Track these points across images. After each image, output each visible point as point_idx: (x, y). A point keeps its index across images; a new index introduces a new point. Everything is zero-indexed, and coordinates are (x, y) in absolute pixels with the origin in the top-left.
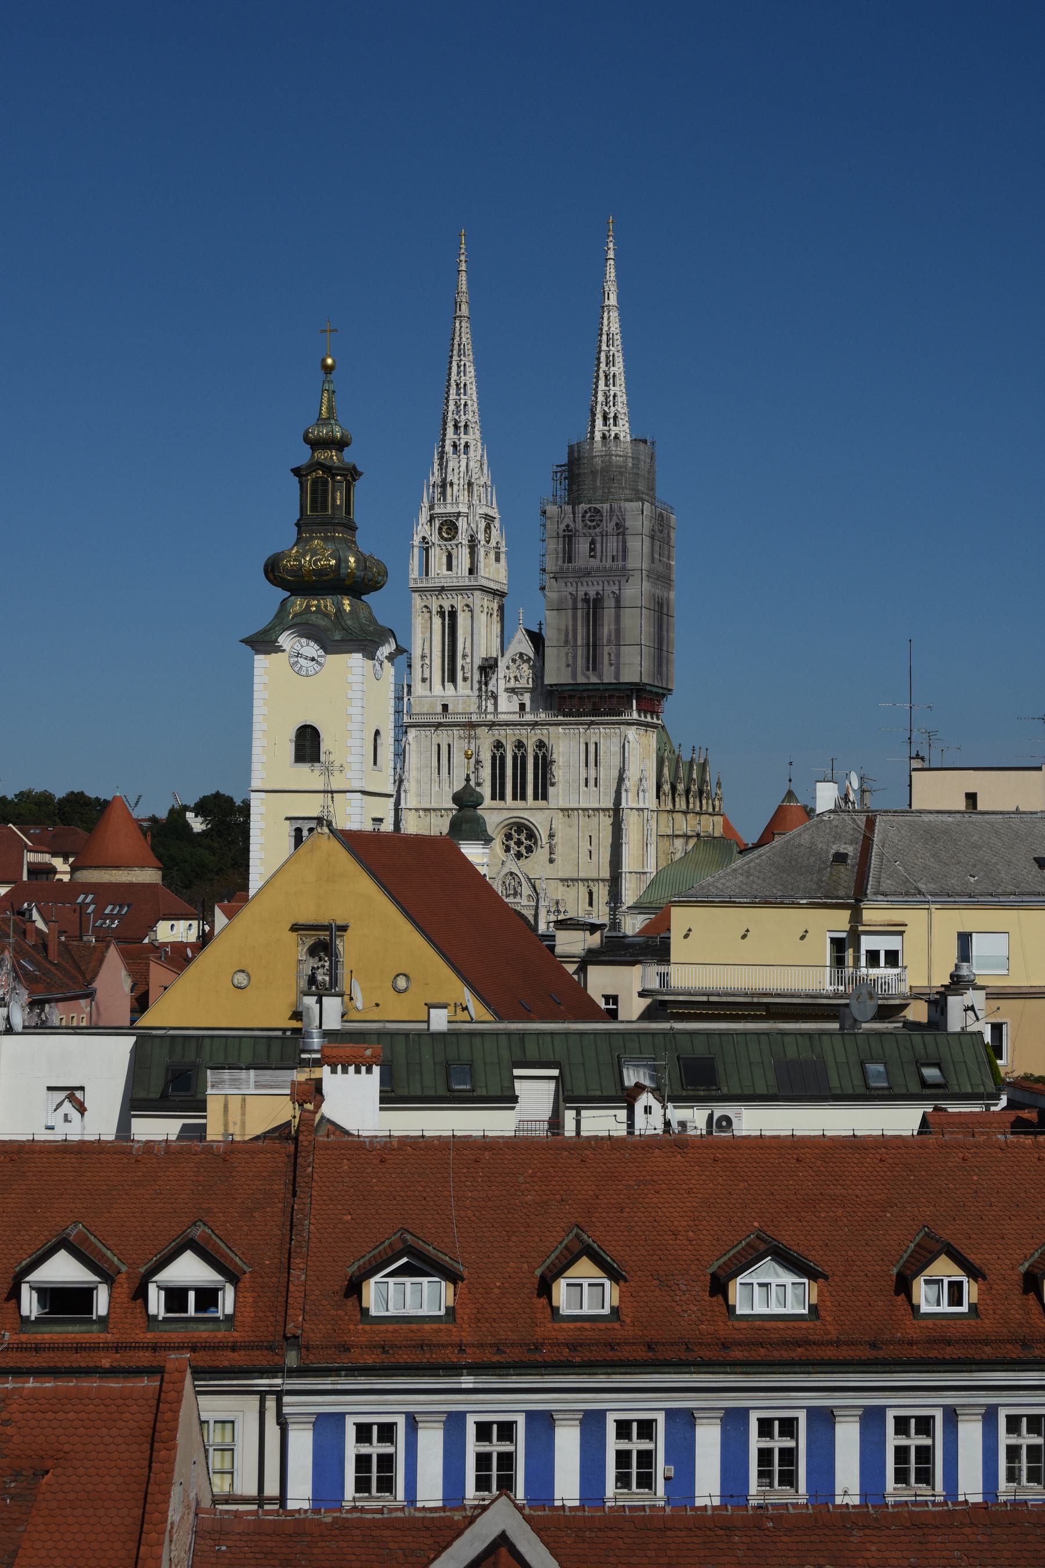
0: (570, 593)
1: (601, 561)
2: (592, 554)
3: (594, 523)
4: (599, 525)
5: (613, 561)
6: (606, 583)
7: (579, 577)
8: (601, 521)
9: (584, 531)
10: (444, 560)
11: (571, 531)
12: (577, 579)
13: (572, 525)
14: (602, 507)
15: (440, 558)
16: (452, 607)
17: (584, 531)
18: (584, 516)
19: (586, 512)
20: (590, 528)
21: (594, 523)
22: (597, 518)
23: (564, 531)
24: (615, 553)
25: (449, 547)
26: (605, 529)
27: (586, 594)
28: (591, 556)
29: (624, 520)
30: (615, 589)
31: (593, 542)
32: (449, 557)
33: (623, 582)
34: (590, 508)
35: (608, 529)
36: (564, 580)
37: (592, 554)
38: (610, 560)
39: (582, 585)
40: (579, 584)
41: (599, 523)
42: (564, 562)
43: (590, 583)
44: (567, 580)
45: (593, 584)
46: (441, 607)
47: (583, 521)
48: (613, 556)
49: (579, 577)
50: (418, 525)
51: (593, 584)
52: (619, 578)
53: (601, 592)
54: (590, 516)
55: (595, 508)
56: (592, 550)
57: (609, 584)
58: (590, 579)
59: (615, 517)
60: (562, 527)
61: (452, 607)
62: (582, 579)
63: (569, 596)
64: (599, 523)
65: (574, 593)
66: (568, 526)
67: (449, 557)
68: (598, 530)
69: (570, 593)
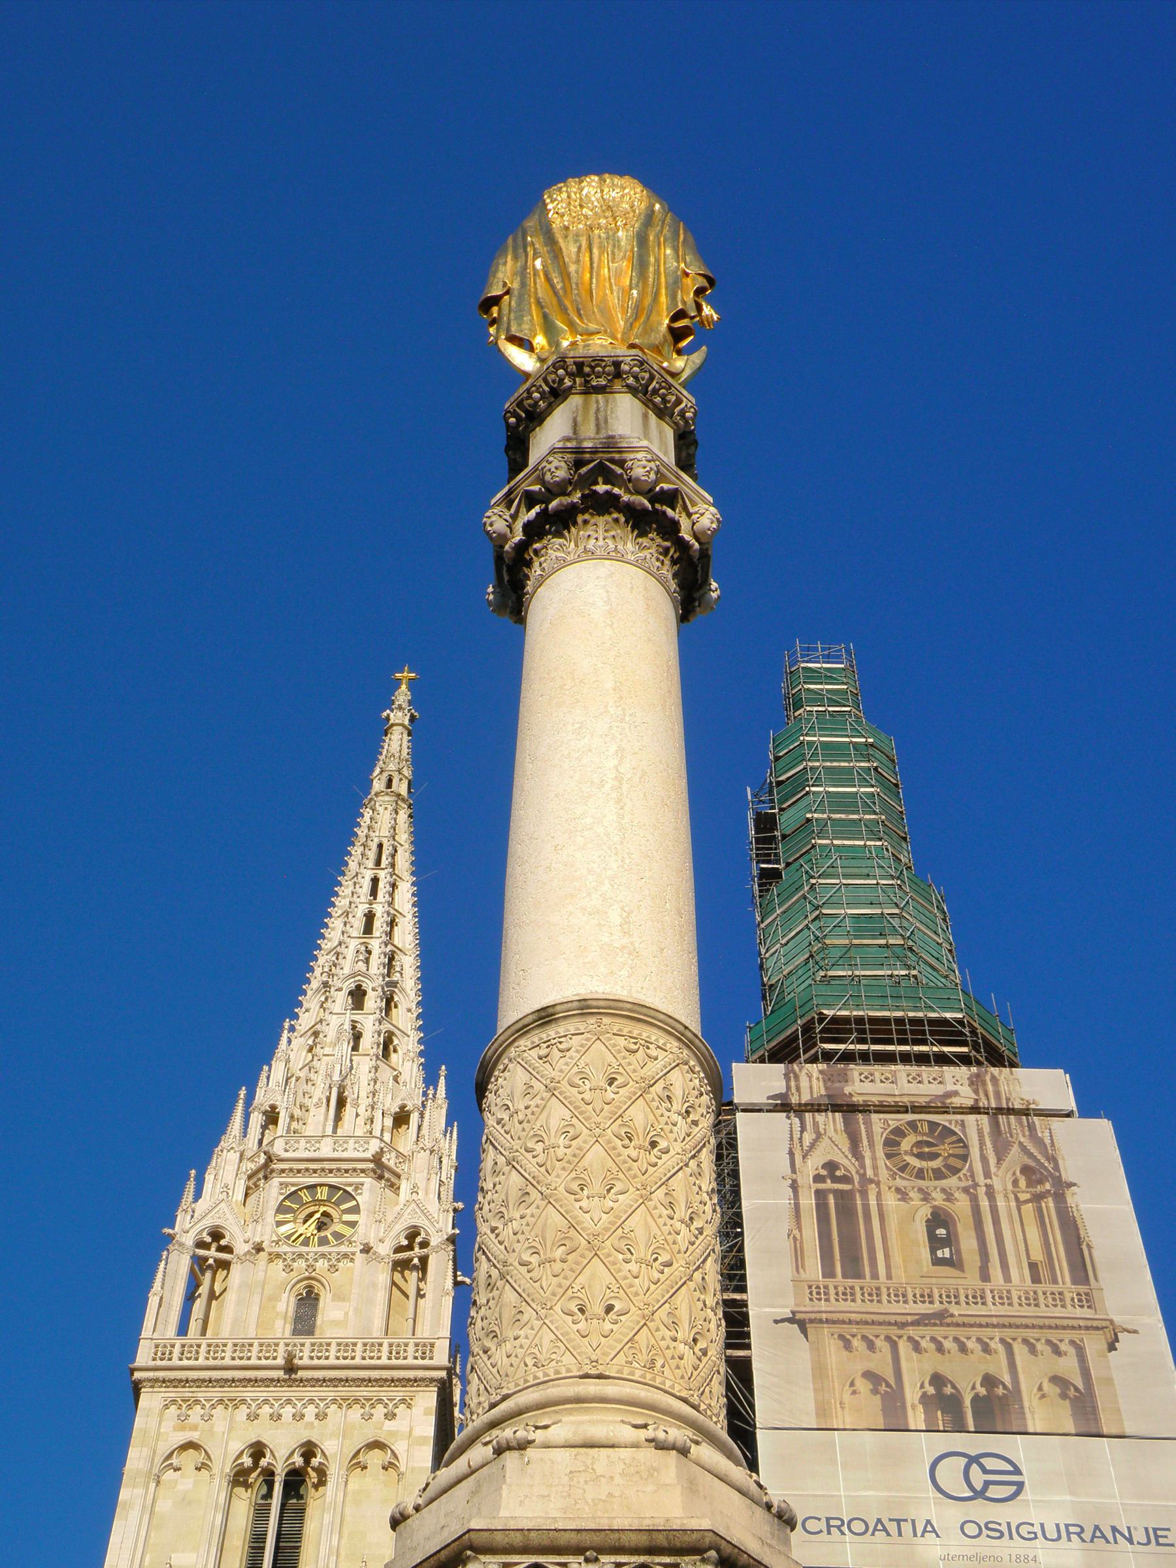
0: (868, 1375)
1: (985, 1276)
2: (941, 1253)
3: (936, 1164)
4: (955, 1171)
5: (1036, 1279)
6: (1019, 1350)
7: (903, 1325)
8: (965, 1158)
9: (899, 1182)
10: (286, 1304)
11: (846, 1179)
12: (893, 1331)
13: (847, 1163)
14: (963, 1124)
15: (274, 1299)
16: (309, 1451)
17: (899, 1182)
18: (891, 1143)
19: (899, 1132)
20: (920, 1174)
21: (936, 1164)
22: (945, 1149)
23: (818, 1178)
24: (1038, 1255)
25: (321, 1265)
26: (981, 1179)
27: (938, 1380)
28: (937, 1262)
29: (1053, 1159)
30: (1068, 1366)
31: (938, 1219)
32: (308, 1301)
33: (1094, 1345)
34: (913, 1125)
35: (997, 1183)
36: (837, 1329)
37: (941, 1253)
38: (1019, 1275)
39: (917, 1347)
40: (904, 1347)
41: (956, 1163)
42: (829, 1273)
43: (948, 1344)
44: (846, 1330)
45: (963, 1349)
46: (258, 1450)
47: (889, 1156)
48: (1033, 1266)
49: (903, 1325)
50: (198, 1195)
51: (963, 1349)
52: (1075, 1335)
53: (1007, 1379)
54: (919, 1144)
55: (933, 1125)
56: (935, 1242)
57: (1033, 1350)
58: (952, 1332)
59: (1015, 1149)
60: (812, 1166)
61: (309, 1451)
62: (911, 1331)
63: (863, 1386)
64: (956, 1163)
65: (888, 1374)
66: (831, 1166)
67: (308, 1301)
68: (952, 1182)
69: (868, 1375)
